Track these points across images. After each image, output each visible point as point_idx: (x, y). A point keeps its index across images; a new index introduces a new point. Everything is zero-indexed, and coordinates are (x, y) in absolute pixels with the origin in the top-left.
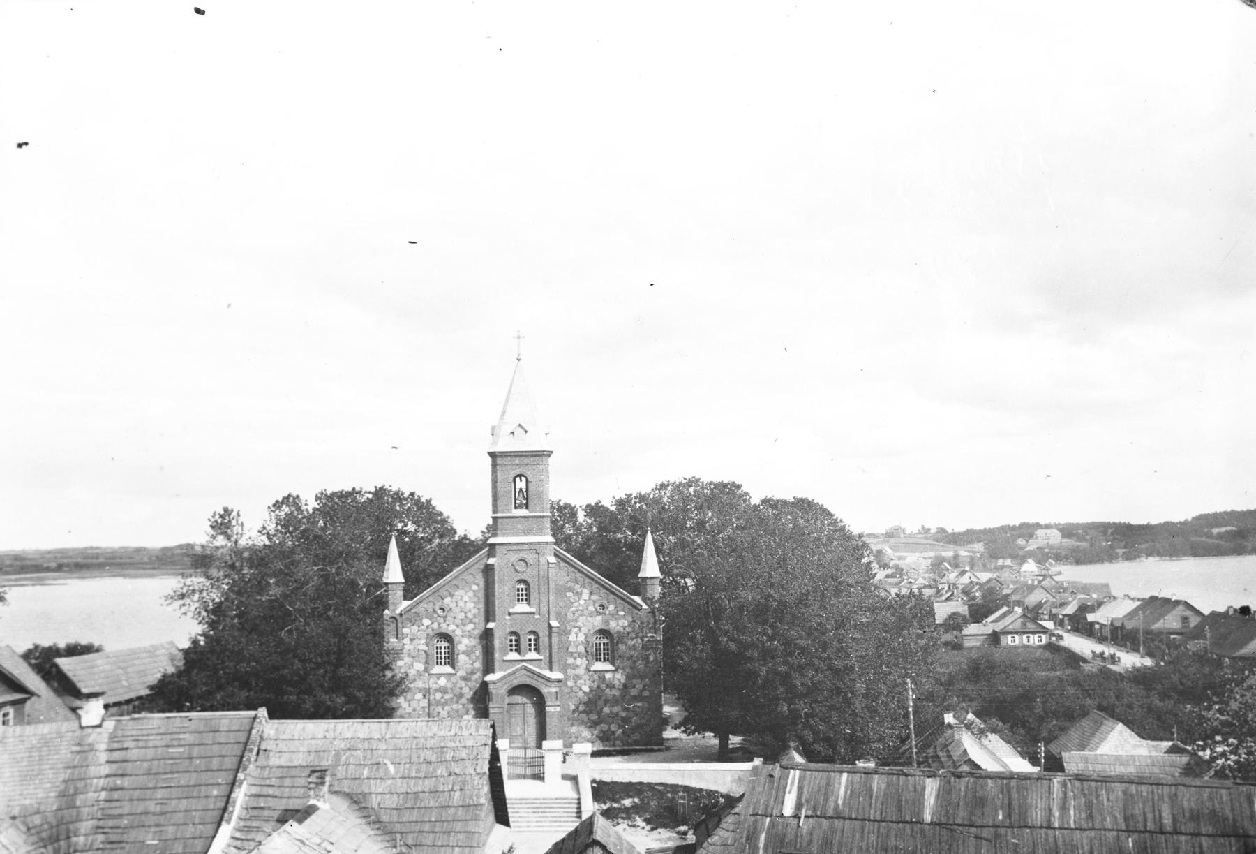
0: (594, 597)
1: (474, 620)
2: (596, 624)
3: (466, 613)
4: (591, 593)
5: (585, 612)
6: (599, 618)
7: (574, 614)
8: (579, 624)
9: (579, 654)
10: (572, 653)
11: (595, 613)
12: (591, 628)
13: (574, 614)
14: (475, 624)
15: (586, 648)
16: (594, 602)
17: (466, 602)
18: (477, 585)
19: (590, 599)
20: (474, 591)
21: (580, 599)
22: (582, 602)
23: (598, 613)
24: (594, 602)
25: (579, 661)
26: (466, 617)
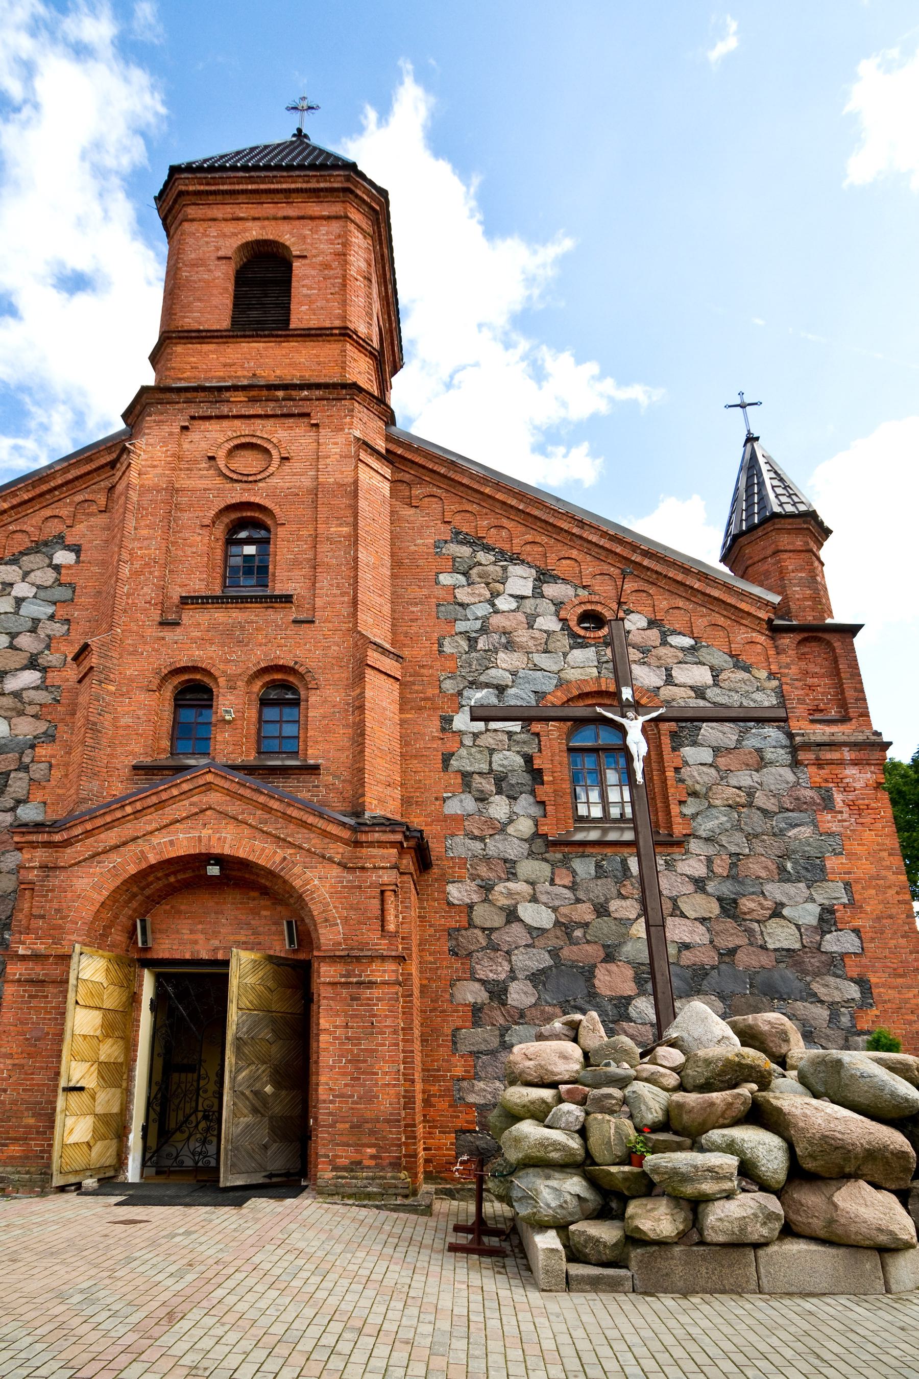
0: (550, 590)
1: (51, 658)
2: (572, 675)
3: (13, 636)
4: (543, 577)
5: (522, 636)
6: (584, 657)
7: (472, 642)
8: (496, 675)
9: (500, 780)
10: (466, 777)
11: (566, 641)
12: (548, 685)
13: (472, 642)
14: (44, 670)
15: (528, 759)
16: (558, 605)
17: (19, 601)
18: (77, 550)
19: (538, 593)
20: (57, 568)
21: (495, 594)
22: (504, 603)
23: (579, 643)
24: (558, 605)
25: (499, 808)
26: (12, 647)
